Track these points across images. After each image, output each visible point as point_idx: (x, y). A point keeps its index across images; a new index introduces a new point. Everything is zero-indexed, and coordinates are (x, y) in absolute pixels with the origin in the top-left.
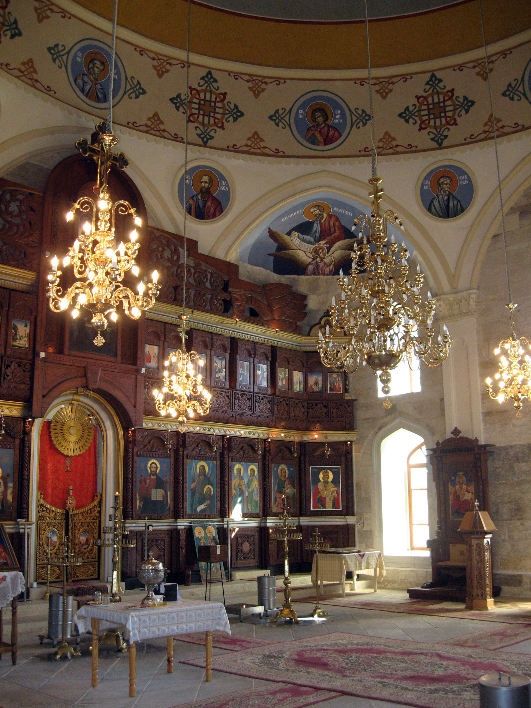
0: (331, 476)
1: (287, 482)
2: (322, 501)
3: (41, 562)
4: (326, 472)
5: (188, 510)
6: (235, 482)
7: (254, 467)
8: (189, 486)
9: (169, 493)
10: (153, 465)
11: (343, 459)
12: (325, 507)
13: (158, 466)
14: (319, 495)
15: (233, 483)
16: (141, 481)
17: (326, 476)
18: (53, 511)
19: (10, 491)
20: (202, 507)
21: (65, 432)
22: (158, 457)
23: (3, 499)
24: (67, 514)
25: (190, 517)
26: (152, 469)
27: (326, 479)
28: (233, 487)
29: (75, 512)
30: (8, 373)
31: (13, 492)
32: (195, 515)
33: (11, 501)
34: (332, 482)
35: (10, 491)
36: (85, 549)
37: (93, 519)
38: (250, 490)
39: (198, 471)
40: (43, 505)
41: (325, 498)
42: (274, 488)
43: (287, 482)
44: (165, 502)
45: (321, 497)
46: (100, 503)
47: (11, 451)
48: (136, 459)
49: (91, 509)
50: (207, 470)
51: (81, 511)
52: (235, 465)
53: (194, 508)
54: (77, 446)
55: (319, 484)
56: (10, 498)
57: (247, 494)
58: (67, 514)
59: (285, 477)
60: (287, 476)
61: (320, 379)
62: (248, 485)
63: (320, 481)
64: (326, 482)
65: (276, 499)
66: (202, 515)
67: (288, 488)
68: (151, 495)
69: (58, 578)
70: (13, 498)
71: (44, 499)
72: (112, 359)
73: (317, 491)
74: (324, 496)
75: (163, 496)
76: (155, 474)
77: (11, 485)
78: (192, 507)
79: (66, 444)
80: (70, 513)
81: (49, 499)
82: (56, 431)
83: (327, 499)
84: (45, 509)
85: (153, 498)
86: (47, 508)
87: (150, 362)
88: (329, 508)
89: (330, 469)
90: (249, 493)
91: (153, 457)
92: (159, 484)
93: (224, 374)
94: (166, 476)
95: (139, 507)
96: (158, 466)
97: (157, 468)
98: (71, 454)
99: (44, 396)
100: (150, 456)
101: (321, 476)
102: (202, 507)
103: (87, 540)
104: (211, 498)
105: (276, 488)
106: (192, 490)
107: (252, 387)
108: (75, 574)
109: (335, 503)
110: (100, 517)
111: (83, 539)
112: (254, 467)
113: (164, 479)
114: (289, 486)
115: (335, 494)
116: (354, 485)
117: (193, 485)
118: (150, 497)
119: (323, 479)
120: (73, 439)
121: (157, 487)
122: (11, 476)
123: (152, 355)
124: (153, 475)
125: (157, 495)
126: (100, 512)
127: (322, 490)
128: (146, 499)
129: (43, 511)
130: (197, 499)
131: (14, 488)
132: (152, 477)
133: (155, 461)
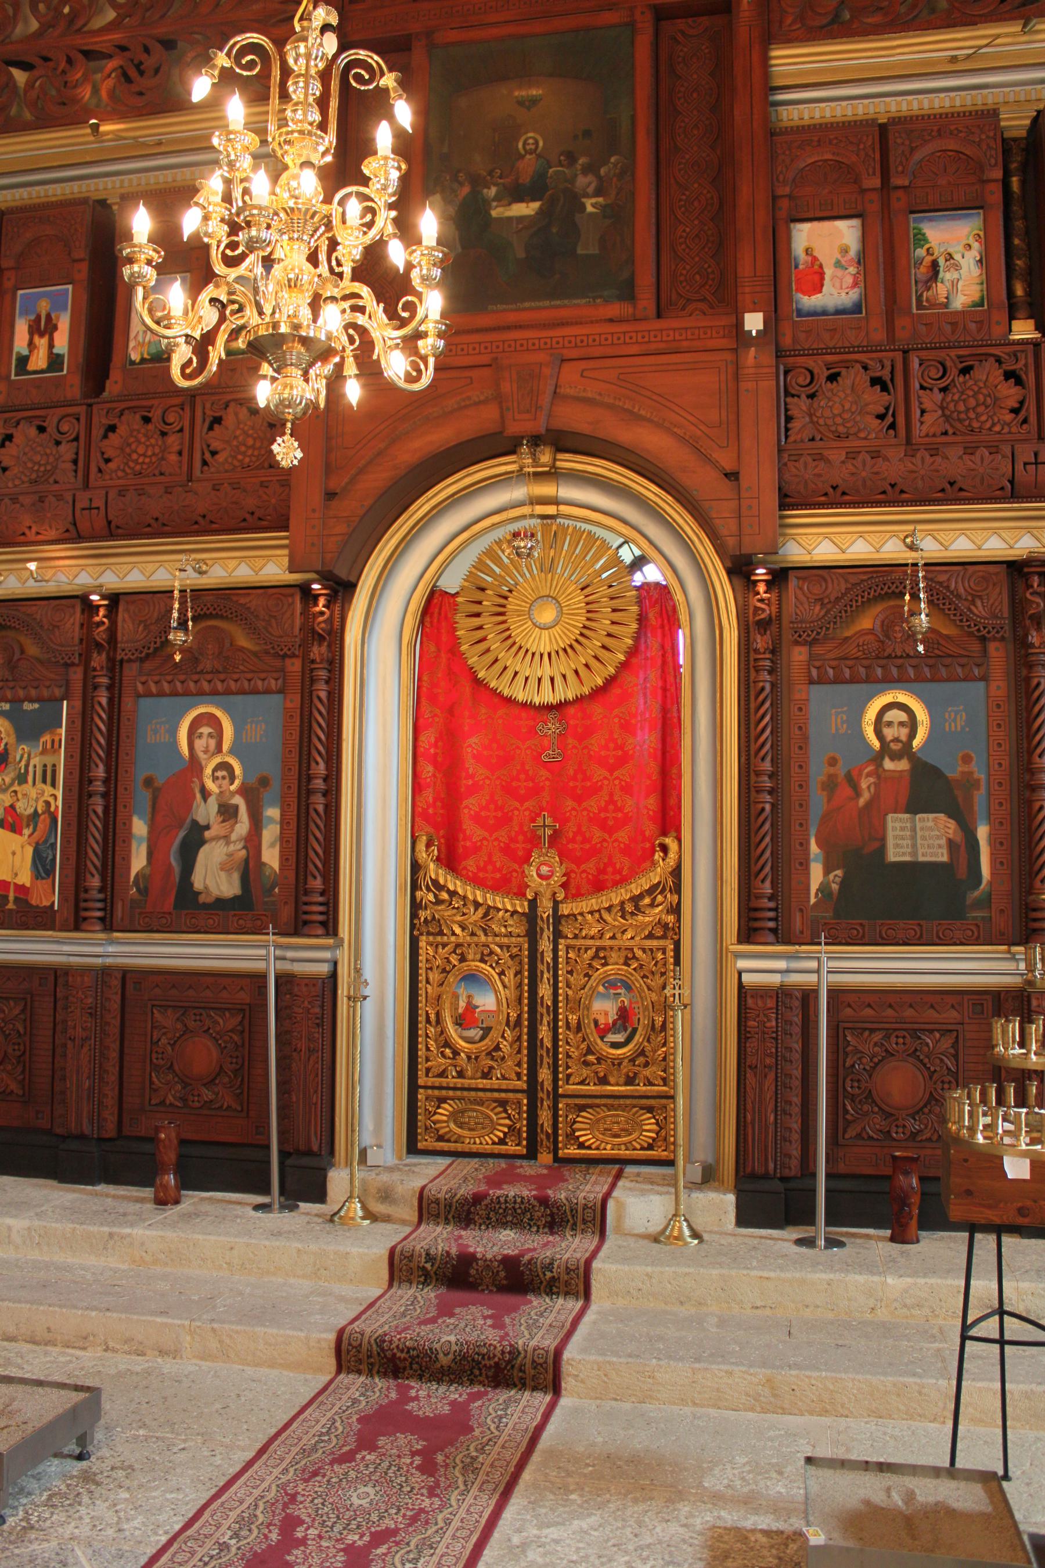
3: (431, 1081)
9: (982, 832)
10: (896, 716)
13: (922, 715)
16: (830, 785)
18: (477, 905)
19: (270, 834)
21: (512, 621)
22: (920, 679)
23: (247, 861)
24: (531, 917)
29: (565, 909)
30: (215, 445)
31: (283, 838)
33: (275, 865)
35: (270, 834)
36: (615, 1045)
37: (650, 936)
40: (435, 882)
44: (962, 872)
46: (677, 872)
47: (277, 698)
48: (800, 692)
49: (636, 899)
51: (593, 903)
54: (564, 665)
56: (271, 857)
58: (531, 917)
68: (883, 839)
69: (502, 1142)
70: (283, 858)
71: (450, 860)
72: (616, 309)
75: (951, 843)
76: (906, 750)
77: (273, 813)
80: (545, 908)
81: (470, 864)
82: (476, 622)
84: (445, 896)
85: (896, 852)
86: (453, 894)
87: (818, 288)
91: (889, 681)
92: (928, 788)
94: (967, 759)
95: (823, 889)
96: (922, 715)
97: (912, 724)
98: (547, 696)
99: (330, 495)
100: (869, 680)
103: (624, 1015)
108: (571, 1137)
110: (677, 929)
111: (605, 1008)
113: (953, 771)
118: (882, 849)
120: (543, 643)
121: (915, 806)
122: (276, 785)
123: (827, 258)
124: (895, 757)
125: (916, 839)
126: (676, 910)
129: (439, 902)
131: (284, 822)
132: (888, 765)
133: (903, 697)
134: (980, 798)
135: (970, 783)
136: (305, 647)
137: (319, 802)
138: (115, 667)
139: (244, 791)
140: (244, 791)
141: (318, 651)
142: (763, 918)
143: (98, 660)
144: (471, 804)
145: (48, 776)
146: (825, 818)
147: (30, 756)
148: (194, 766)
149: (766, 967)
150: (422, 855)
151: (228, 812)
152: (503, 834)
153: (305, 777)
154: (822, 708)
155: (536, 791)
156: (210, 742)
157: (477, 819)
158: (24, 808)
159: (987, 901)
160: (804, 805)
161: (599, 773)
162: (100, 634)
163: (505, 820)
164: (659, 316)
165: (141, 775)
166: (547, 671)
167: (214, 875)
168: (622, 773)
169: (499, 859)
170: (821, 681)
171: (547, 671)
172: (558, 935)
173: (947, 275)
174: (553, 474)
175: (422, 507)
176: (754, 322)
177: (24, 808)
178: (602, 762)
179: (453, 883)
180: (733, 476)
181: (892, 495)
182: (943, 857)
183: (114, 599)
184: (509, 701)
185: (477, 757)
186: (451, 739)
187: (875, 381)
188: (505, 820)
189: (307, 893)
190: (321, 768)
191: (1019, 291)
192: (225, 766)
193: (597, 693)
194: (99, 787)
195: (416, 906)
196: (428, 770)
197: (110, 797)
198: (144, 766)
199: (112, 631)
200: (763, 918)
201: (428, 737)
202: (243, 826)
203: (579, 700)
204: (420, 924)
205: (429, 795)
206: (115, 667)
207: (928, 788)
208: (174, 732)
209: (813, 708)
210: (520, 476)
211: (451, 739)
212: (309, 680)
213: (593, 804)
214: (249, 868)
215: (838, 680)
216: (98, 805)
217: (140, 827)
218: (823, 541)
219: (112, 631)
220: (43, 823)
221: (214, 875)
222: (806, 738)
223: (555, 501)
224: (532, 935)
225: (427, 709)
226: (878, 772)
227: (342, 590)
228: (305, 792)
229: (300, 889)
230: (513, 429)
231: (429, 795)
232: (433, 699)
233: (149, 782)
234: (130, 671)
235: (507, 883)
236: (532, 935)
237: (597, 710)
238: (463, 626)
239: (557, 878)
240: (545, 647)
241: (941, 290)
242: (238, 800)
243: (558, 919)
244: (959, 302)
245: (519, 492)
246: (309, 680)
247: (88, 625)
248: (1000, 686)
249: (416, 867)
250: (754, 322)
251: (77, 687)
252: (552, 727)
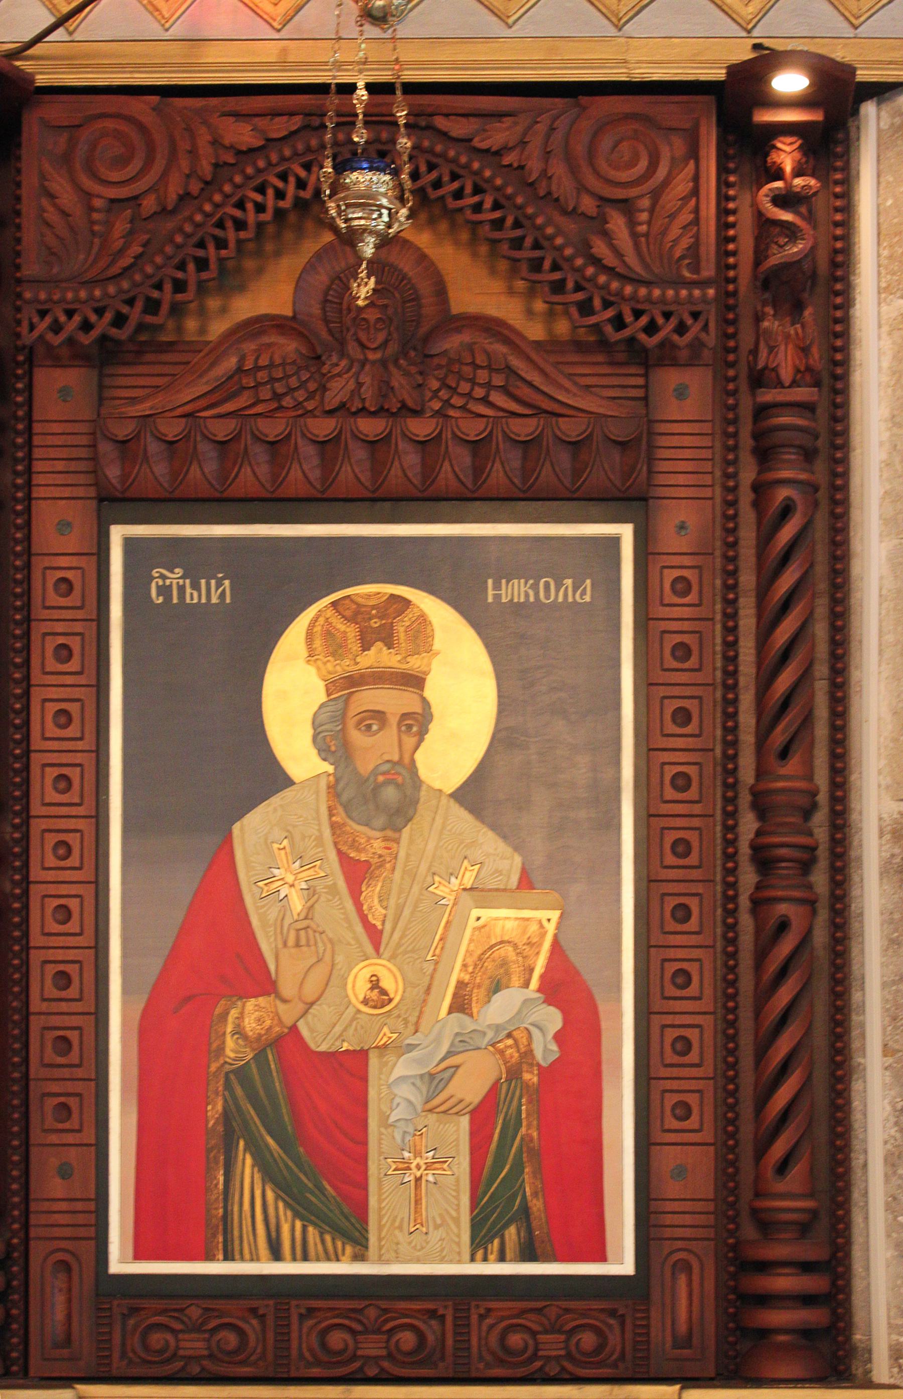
0: (462, 691)
2: (312, 1114)
4: (380, 625)
11: (685, 400)
12: (353, 1232)
14: (252, 1016)
17: (375, 706)
27: (374, 750)
34: (473, 794)
45: (287, 1042)
55: (253, 832)
63: (275, 779)
64: (376, 797)
73: (219, 951)
74: (322, 1034)
83: (393, 1094)
88: (423, 1230)
89: (457, 577)
101: (292, 690)
109: (527, 1150)
115: (522, 1012)
116: (872, 850)
119: (331, 738)
127: (305, 933)
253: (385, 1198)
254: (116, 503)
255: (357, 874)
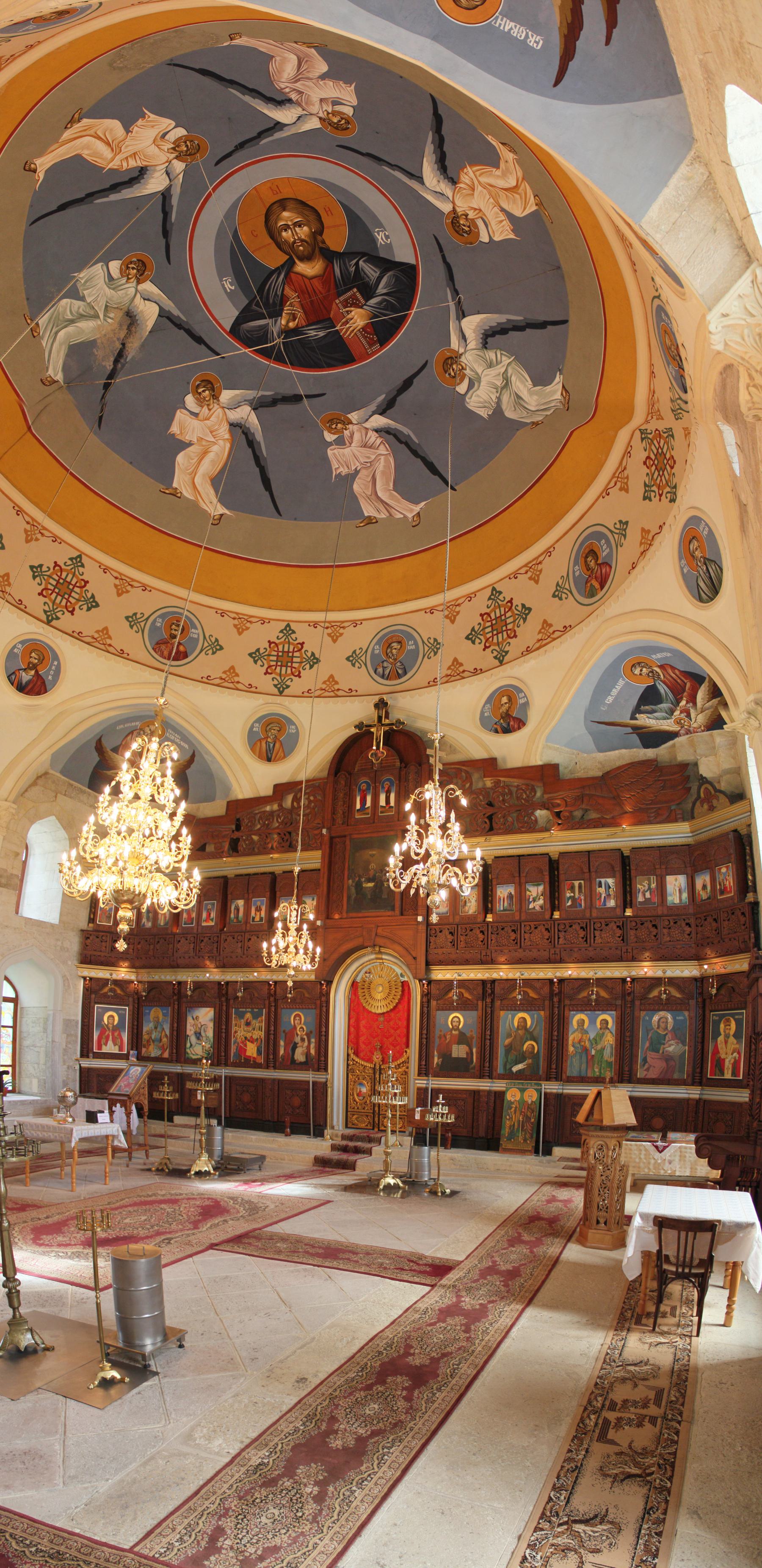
1: (669, 1036)
5: (500, 1070)
6: (573, 1037)
7: (609, 1017)
8: (503, 1041)
9: (474, 1050)
10: (456, 1019)
15: (571, 1038)
16: (440, 1037)
19: (312, 1045)
20: (520, 1066)
24: (374, 1069)
25: (501, 1077)
26: (454, 1024)
28: (570, 1042)
31: (315, 1047)
32: (508, 1075)
35: (312, 1045)
38: (599, 1047)
39: (516, 1024)
41: (724, 1060)
42: (643, 1045)
43: (669, 1036)
47: (314, 1011)
49: (399, 1065)
50: (529, 1023)
52: (574, 1015)
53: (508, 1067)
54: (383, 1003)
56: (313, 1051)
57: (593, 1052)
59: (666, 1028)
60: (670, 1027)
61: (707, 878)
62: (596, 1041)
65: (645, 1060)
66: (520, 1076)
67: (670, 1046)
71: (356, 1053)
72: (390, 913)
74: (723, 1056)
75: (467, 1053)
76: (458, 1029)
77: (313, 1040)
78: (505, 1066)
79: (372, 1002)
80: (378, 1067)
81: (362, 1054)
85: (455, 1054)
90: (597, 1051)
93: (541, 902)
98: (379, 1011)
101: (722, 1026)
102: (520, 1066)
104: (535, 1057)
105: (647, 1044)
106: (505, 1046)
107: (588, 911)
112: (609, 1017)
113: (468, 1034)
114: (672, 1042)
117: (507, 1041)
118: (451, 1054)
120: (379, 996)
125: (459, 1051)
128: (446, 1056)
130: (512, 1057)
132: (453, 1032)
134: (474, 1041)
135: (472, 1038)
136: (320, 997)
137: (323, 1038)
138: (276, 1001)
139: (307, 1034)
140: (307, 1034)
141: (323, 999)
142: (424, 1070)
143: (272, 999)
144: (362, 1039)
145: (260, 1029)
146: (439, 1045)
147: (255, 1023)
148: (295, 1028)
149: (422, 1083)
150: (350, 1052)
151: (303, 1040)
152: (369, 1047)
153: (320, 1032)
154: (439, 1015)
155: (377, 1036)
156: (298, 1020)
157: (364, 1043)
158: (255, 1037)
159: (474, 1068)
160: (434, 1042)
161: (392, 1031)
162: (272, 992)
163: (370, 1043)
164: (402, 914)
165: (282, 1029)
166: (380, 1004)
167: (299, 1056)
168: (398, 1031)
169: (369, 1054)
170: (438, 1010)
171: (380, 1004)
172: (380, 1073)
173: (468, 904)
174: (380, 952)
175: (349, 961)
176: (420, 919)
177: (255, 1037)
178: (393, 1028)
179: (357, 1060)
180: (415, 958)
181: (453, 963)
182: (465, 1056)
183: (276, 982)
184: (370, 1012)
185: (364, 1027)
186: (358, 1021)
187: (451, 933)
188: (370, 1043)
189: (320, 1061)
190: (324, 1029)
191: (490, 906)
192: (302, 1028)
193: (392, 1010)
194: (272, 1032)
195: (348, 1065)
196: (352, 1029)
197: (275, 1034)
198: (283, 1027)
199: (275, 991)
200: (424, 1070)
201: (352, 1021)
202: (306, 1044)
203: (388, 1012)
204: (349, 1070)
205: (352, 1036)
206: (276, 1001)
207: (462, 1038)
208: (290, 1019)
209: (438, 1017)
210: (372, 953)
211: (358, 1021)
212: (321, 1006)
213: (391, 1040)
214: (308, 1055)
215: (443, 1010)
216: (272, 1037)
217: (282, 1043)
218: (441, 974)
219: (275, 991)
220: (259, 1041)
221: (299, 1056)
222: (435, 1025)
223: (382, 959)
224: (374, 1073)
225: (352, 1013)
226: (451, 1034)
227: (329, 983)
228: (320, 1036)
229: (319, 1060)
230: (366, 944)
231: (352, 1036)
232: (354, 1010)
233: (284, 1031)
234: (280, 1002)
235: (369, 1060)
236: (374, 1073)
237: (392, 1015)
238: (360, 991)
239: (380, 1059)
240: (379, 998)
241: (467, 908)
242: (305, 1037)
243: (380, 1069)
244: (471, 912)
245: (373, 956)
246: (321, 1006)
247: (269, 989)
248: (480, 1011)
249: (348, 1055)
250: (420, 919)
251: (267, 1005)
252: (381, 1019)
253: (726, 1071)
254: (711, 1011)
255: (726, 1042)
